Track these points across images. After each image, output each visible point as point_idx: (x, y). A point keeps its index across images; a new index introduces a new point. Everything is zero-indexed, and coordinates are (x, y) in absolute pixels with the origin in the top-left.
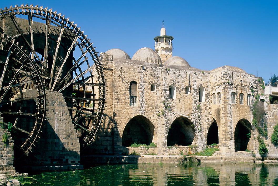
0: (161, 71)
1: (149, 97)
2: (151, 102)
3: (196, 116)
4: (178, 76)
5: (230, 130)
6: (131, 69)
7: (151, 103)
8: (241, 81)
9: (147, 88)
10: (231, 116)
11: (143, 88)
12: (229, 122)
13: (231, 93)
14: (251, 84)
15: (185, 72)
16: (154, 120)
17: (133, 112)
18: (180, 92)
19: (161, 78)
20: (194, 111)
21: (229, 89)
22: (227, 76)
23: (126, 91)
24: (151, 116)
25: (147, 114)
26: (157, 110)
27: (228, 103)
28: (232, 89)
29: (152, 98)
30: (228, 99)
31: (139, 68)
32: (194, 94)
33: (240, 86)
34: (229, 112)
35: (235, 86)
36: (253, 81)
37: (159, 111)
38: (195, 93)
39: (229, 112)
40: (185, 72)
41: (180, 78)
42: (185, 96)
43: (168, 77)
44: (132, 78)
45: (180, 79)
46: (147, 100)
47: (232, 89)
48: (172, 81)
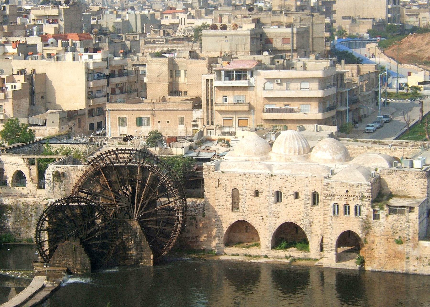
0: (265, 178)
1: (252, 203)
2: (254, 208)
3: (306, 222)
5: (330, 242)
6: (232, 178)
7: (254, 209)
8: (347, 191)
9: (250, 195)
11: (245, 195)
13: (332, 205)
14: (361, 193)
15: (295, 177)
16: (257, 225)
17: (235, 217)
19: (265, 184)
20: (305, 217)
21: (329, 201)
22: (328, 188)
23: (227, 199)
24: (254, 221)
25: (250, 219)
26: (261, 215)
27: (329, 215)
28: (334, 200)
29: (255, 204)
30: (327, 210)
31: (241, 176)
32: (305, 199)
33: (346, 197)
34: (329, 224)
35: (339, 197)
36: (365, 191)
37: (262, 216)
38: (306, 198)
39: (329, 224)
40: (295, 177)
41: (288, 183)
42: (293, 202)
43: (273, 183)
44: (233, 186)
45: (288, 184)
46: (250, 206)
47: (334, 200)
48: (278, 187)
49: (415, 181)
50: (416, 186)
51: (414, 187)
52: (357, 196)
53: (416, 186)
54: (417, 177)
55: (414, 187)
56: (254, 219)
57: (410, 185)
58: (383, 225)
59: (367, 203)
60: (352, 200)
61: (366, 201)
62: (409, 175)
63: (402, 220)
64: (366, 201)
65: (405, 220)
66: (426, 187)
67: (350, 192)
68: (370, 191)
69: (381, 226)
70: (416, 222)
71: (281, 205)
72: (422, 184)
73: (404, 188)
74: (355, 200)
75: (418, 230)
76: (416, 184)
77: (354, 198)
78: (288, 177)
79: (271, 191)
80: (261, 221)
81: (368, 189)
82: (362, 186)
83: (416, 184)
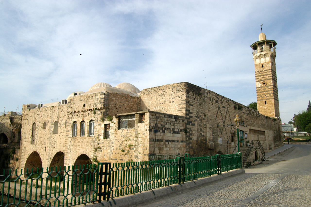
4: (61, 111)
8: (84, 105)
10: (71, 151)
12: (68, 159)
18: (61, 126)
26: (45, 146)
34: (69, 148)
36: (99, 101)
39: (69, 148)
49: (172, 97)
50: (173, 102)
51: (172, 103)
52: (91, 110)
53: (173, 102)
54: (175, 91)
55: (172, 103)
56: (41, 150)
57: (167, 102)
58: (112, 145)
59: (99, 115)
60: (87, 115)
61: (99, 114)
62: (166, 91)
63: (131, 136)
64: (99, 114)
65: (134, 134)
66: (184, 102)
67: (86, 105)
68: (102, 101)
69: (110, 147)
70: (146, 136)
71: (57, 135)
72: (180, 99)
73: (162, 107)
74: (90, 115)
75: (148, 148)
76: (174, 100)
77: (89, 112)
78: (63, 107)
79: (52, 122)
80: (45, 151)
81: (101, 99)
82: (96, 96)
83: (174, 100)
